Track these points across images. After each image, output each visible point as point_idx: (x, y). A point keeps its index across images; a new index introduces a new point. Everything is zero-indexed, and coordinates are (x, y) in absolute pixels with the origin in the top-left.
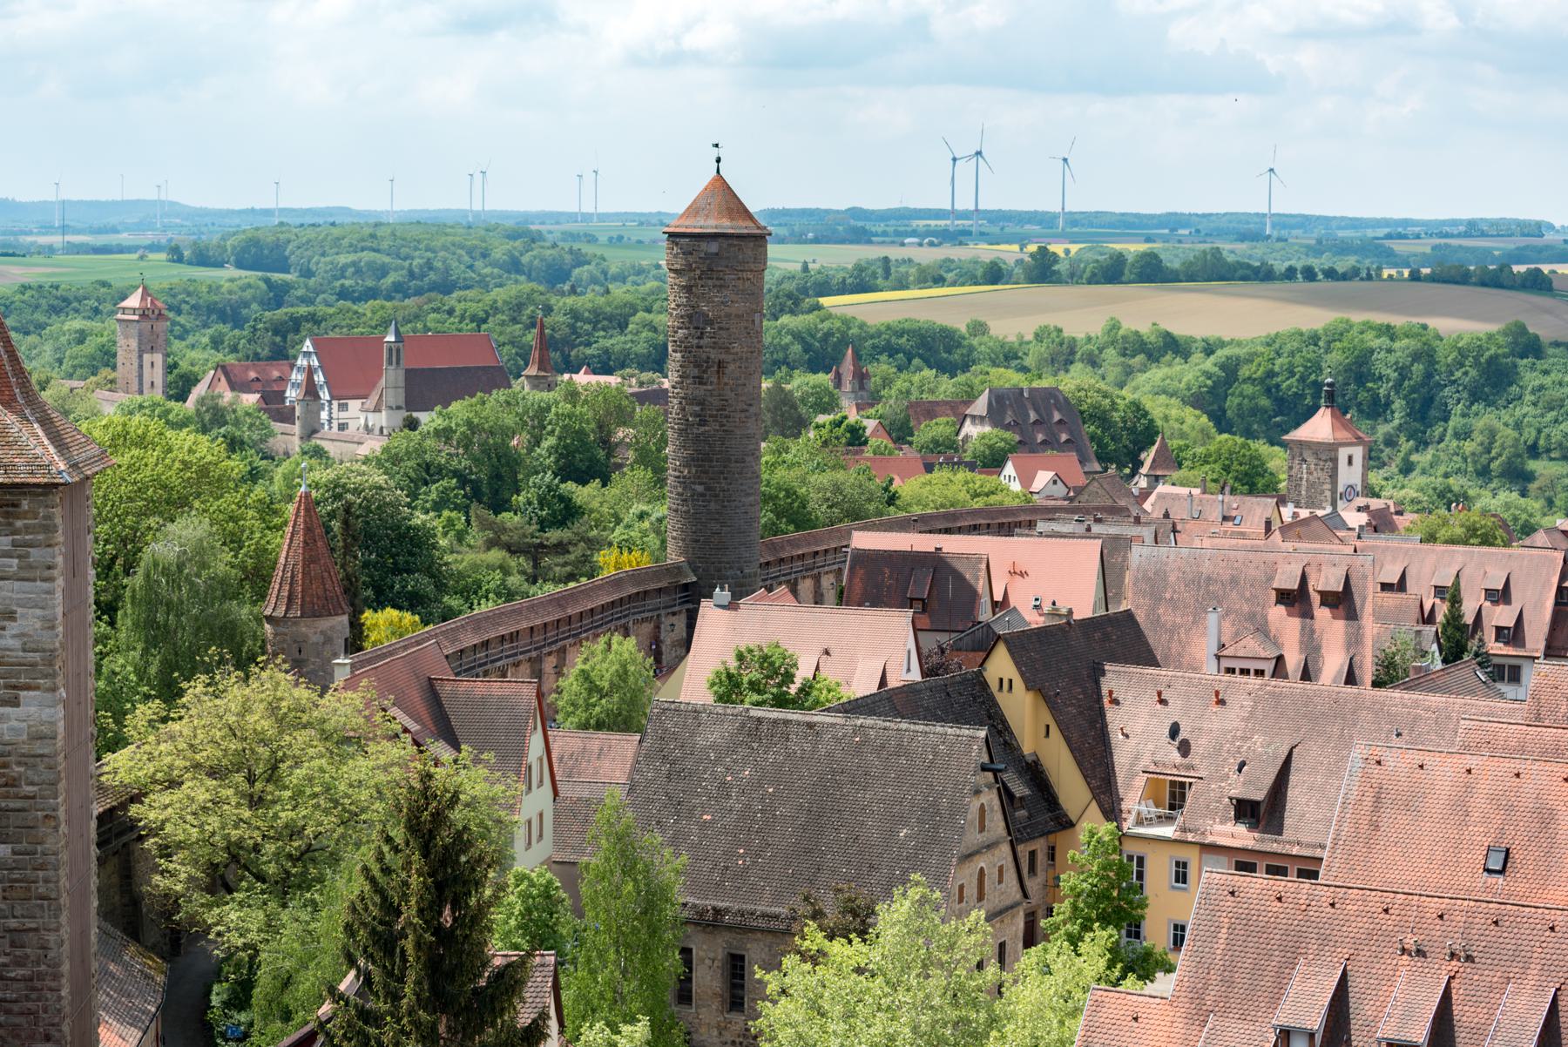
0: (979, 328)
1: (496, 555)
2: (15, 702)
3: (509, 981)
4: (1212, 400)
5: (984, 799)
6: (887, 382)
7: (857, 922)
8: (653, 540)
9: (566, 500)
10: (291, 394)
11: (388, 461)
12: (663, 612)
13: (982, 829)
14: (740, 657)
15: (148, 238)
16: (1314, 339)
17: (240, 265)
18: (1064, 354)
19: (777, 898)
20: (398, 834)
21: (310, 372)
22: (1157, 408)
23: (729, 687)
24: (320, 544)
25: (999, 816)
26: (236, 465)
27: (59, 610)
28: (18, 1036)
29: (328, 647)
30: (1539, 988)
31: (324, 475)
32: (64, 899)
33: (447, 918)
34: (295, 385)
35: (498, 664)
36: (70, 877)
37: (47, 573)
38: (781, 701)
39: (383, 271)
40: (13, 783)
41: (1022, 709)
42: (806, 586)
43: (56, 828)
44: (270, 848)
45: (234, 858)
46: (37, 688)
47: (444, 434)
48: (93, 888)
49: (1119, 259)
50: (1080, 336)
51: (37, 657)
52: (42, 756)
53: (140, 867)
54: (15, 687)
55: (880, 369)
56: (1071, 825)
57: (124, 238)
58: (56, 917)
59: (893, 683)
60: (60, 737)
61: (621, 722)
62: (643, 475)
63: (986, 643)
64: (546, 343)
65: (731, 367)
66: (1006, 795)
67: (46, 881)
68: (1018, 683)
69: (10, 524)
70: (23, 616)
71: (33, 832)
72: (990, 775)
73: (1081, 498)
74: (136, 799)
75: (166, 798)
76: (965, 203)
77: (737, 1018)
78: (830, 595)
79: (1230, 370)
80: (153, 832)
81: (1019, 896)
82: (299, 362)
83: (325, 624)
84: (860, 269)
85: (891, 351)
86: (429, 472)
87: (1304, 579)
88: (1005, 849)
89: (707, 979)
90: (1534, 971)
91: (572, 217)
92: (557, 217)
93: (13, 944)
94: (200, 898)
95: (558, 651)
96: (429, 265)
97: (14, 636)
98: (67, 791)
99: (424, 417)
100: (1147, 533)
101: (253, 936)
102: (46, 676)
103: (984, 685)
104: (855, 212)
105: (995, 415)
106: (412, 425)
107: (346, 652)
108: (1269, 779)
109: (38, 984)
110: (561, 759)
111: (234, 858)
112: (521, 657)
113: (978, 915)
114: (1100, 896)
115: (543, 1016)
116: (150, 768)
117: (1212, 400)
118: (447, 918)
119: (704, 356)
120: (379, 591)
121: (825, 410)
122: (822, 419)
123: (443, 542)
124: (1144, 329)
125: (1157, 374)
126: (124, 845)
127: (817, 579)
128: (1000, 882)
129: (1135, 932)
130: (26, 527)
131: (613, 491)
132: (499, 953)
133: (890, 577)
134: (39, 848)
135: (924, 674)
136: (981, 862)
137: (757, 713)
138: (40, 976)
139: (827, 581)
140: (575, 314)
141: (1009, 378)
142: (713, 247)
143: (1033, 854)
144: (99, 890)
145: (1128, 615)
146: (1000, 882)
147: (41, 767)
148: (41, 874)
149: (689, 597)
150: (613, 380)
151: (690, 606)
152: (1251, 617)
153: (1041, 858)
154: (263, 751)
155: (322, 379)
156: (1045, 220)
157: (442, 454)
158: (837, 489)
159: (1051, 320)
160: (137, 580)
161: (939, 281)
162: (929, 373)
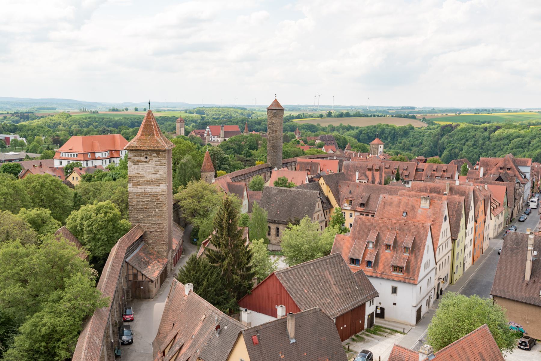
0: (318, 125)
1: (239, 162)
2: (159, 186)
3: (240, 232)
4: (358, 137)
6: (303, 134)
7: (297, 222)
8: (265, 160)
9: (250, 153)
10: (205, 135)
11: (221, 146)
14: (279, 179)
15: (181, 109)
16: (375, 127)
17: (197, 113)
18: (333, 129)
19: (285, 218)
20: (223, 207)
21: (208, 131)
22: (348, 138)
23: (277, 184)
26: (196, 146)
30: (412, 236)
31: (211, 148)
33: (231, 221)
38: (285, 186)
39: (220, 115)
40: (159, 199)
41: (325, 188)
42: (290, 167)
44: (202, 209)
45: (195, 211)
47: (231, 142)
49: (342, 113)
50: (336, 126)
53: (180, 213)
55: (303, 131)
57: (177, 109)
59: (304, 184)
61: (260, 189)
62: (263, 149)
63: (319, 177)
64: (248, 127)
66: (322, 202)
68: (325, 184)
74: (179, 201)
75: (184, 201)
76: (317, 104)
77: (277, 238)
78: (294, 169)
79: (361, 132)
80: (182, 207)
83: (211, 173)
84: (299, 115)
85: (304, 128)
86: (228, 148)
87: (373, 167)
89: (273, 231)
90: (411, 233)
91: (252, 106)
92: (249, 106)
94: (190, 218)
96: (228, 114)
99: (227, 139)
100: (346, 159)
101: (198, 224)
104: (299, 106)
105: (322, 139)
106: (225, 140)
108: (366, 200)
111: (195, 211)
113: (317, 222)
114: (338, 219)
115: (246, 238)
116: (182, 196)
117: (358, 137)
118: (231, 221)
120: (220, 167)
121: (293, 138)
122: (293, 140)
123: (230, 160)
124: (346, 125)
125: (348, 132)
129: (343, 224)
131: (258, 151)
132: (239, 228)
136: (318, 213)
137: (282, 188)
139: (293, 167)
140: (251, 122)
141: (323, 133)
142: (275, 111)
145: (343, 173)
149: (271, 169)
150: (258, 133)
152: (364, 173)
153: (328, 212)
154: (200, 194)
156: (330, 107)
157: (230, 145)
158: (295, 151)
159: (331, 124)
160: (179, 165)
161: (312, 117)
162: (310, 132)
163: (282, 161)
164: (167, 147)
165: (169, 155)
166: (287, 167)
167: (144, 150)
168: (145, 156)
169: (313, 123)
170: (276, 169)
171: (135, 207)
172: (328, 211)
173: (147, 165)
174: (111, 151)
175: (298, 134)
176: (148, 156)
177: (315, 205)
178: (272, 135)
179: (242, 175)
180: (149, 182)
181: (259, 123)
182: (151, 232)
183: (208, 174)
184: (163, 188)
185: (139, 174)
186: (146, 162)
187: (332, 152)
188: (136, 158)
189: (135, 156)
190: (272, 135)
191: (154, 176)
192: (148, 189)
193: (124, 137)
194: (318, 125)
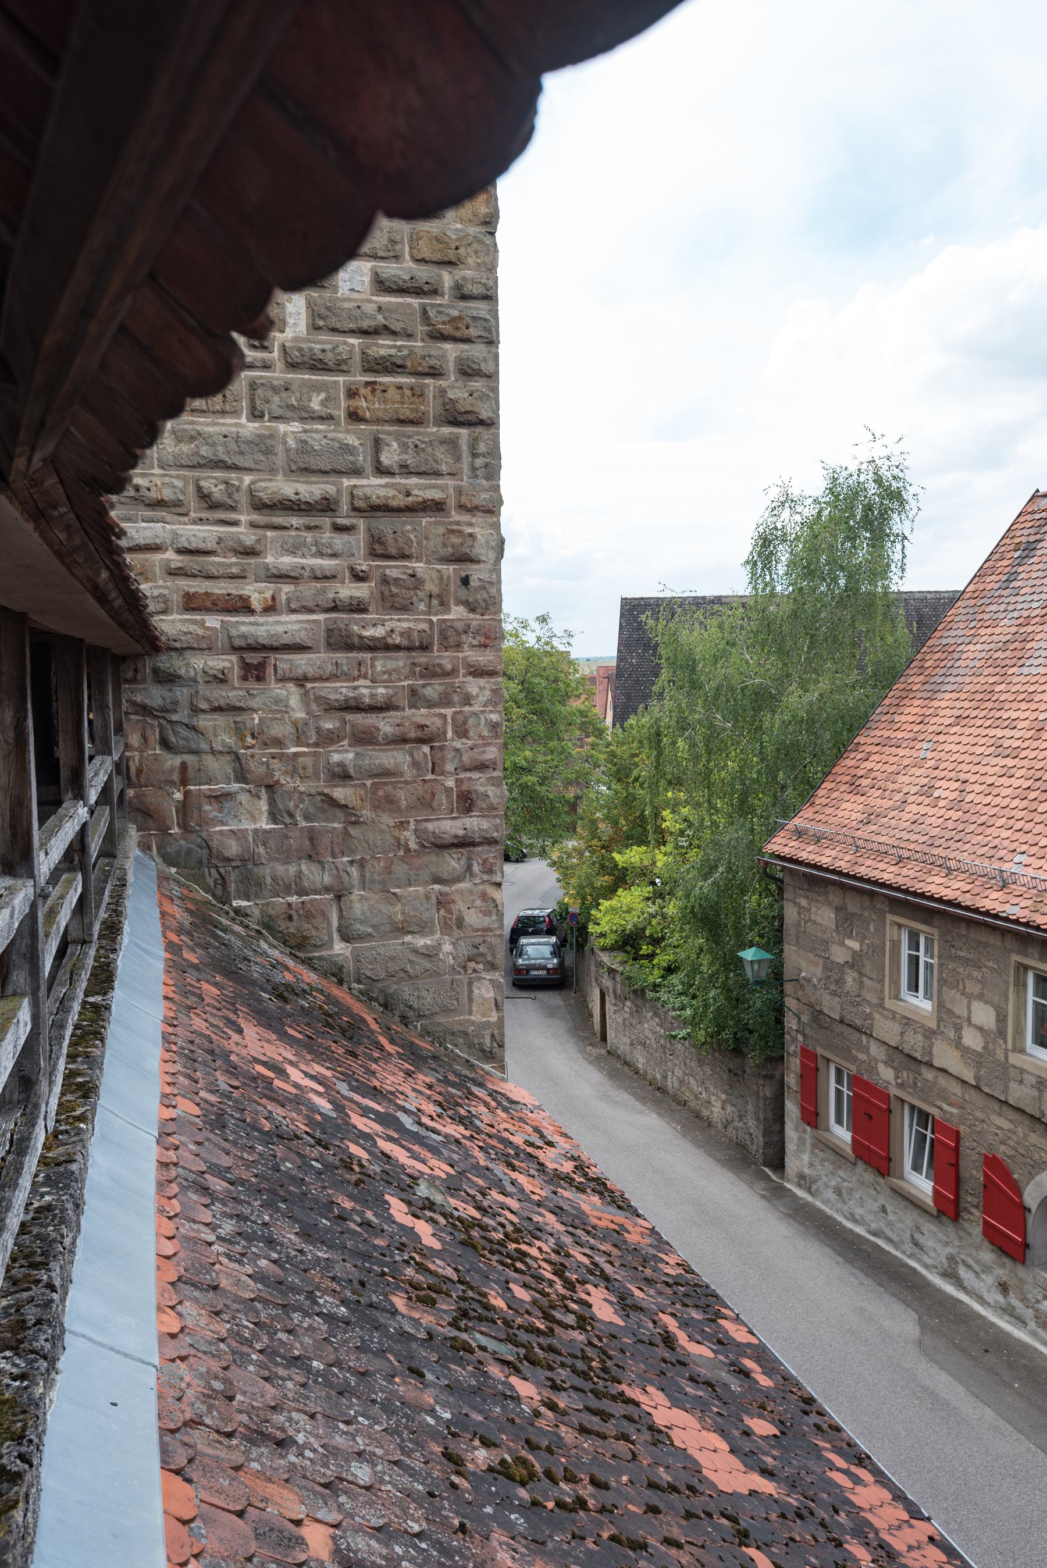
28: (390, 803)
93: (378, 549)
109: (445, 659)
134: (447, 278)
138: (450, 637)
182: (256, 660)
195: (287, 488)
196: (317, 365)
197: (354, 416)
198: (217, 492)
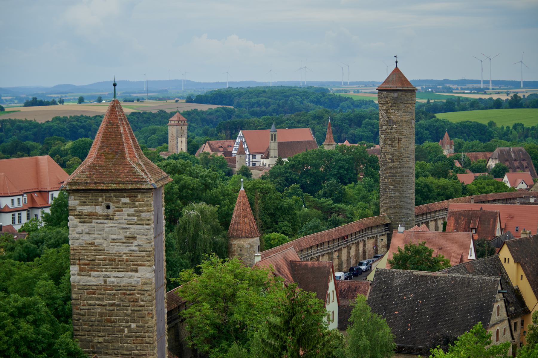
2: (136, 271)
5: (499, 304)
12: (378, 235)
13: (498, 315)
24: (248, 210)
25: (504, 310)
27: (153, 236)
29: (252, 249)
32: (156, 344)
34: (235, 149)
35: (316, 255)
36: (157, 335)
37: (147, 222)
40: (136, 301)
43: (152, 318)
46: (144, 265)
48: (166, 340)
51: (144, 254)
52: (146, 291)
54: (136, 265)
56: (529, 312)
58: (153, 350)
60: (153, 284)
65: (403, 140)
67: (149, 337)
68: (512, 260)
69: (134, 204)
70: (139, 238)
71: (144, 319)
72: (501, 295)
73: (532, 189)
81: (510, 339)
82: (237, 140)
83: (250, 240)
88: (506, 322)
95: (339, 250)
97: (136, 246)
98: (156, 304)
102: (148, 261)
103: (499, 261)
107: (258, 251)
110: (341, 291)
112: (325, 252)
119: (393, 136)
126: (176, 324)
127: (436, 221)
128: (504, 334)
130: (140, 205)
133: (463, 220)
134: (146, 325)
135: (477, 257)
136: (498, 327)
143: (516, 323)
144: (168, 340)
146: (504, 334)
147: (146, 295)
148: (147, 334)
151: (389, 232)
153: (519, 325)
155: (246, 146)
163: (414, 210)
164: (152, 182)
165: (157, 201)
166: (427, 224)
167: (102, 191)
168: (105, 203)
169: (480, 121)
170: (401, 229)
171: (86, 318)
172: (519, 320)
173: (110, 223)
174: (30, 193)
175: (448, 146)
176: (111, 204)
177: (491, 308)
178: (391, 150)
179: (322, 244)
180: (115, 263)
181: (358, 121)
183: (245, 243)
184: (146, 275)
185: (92, 244)
186: (107, 217)
187: (524, 186)
188: (87, 209)
189: (84, 204)
190: (391, 150)
191: (124, 249)
192: (112, 279)
193: (57, 161)
194: (491, 124)
195: (125, 352)
196: (129, 337)
197: (134, 343)
198: (116, 353)
